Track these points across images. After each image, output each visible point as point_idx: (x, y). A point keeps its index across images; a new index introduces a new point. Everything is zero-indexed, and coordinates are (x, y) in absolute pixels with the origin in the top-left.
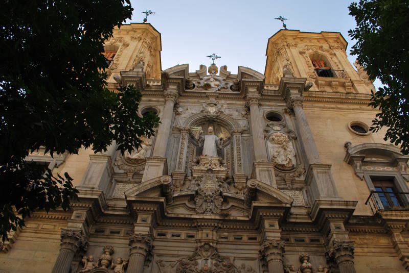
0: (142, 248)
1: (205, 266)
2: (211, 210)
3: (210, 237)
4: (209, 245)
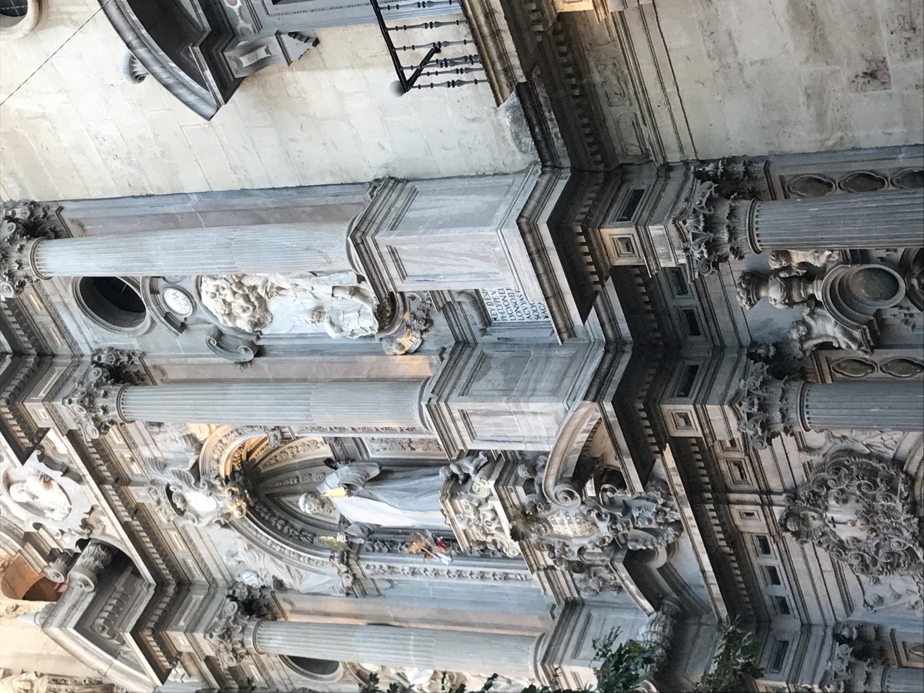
2: (657, 514)
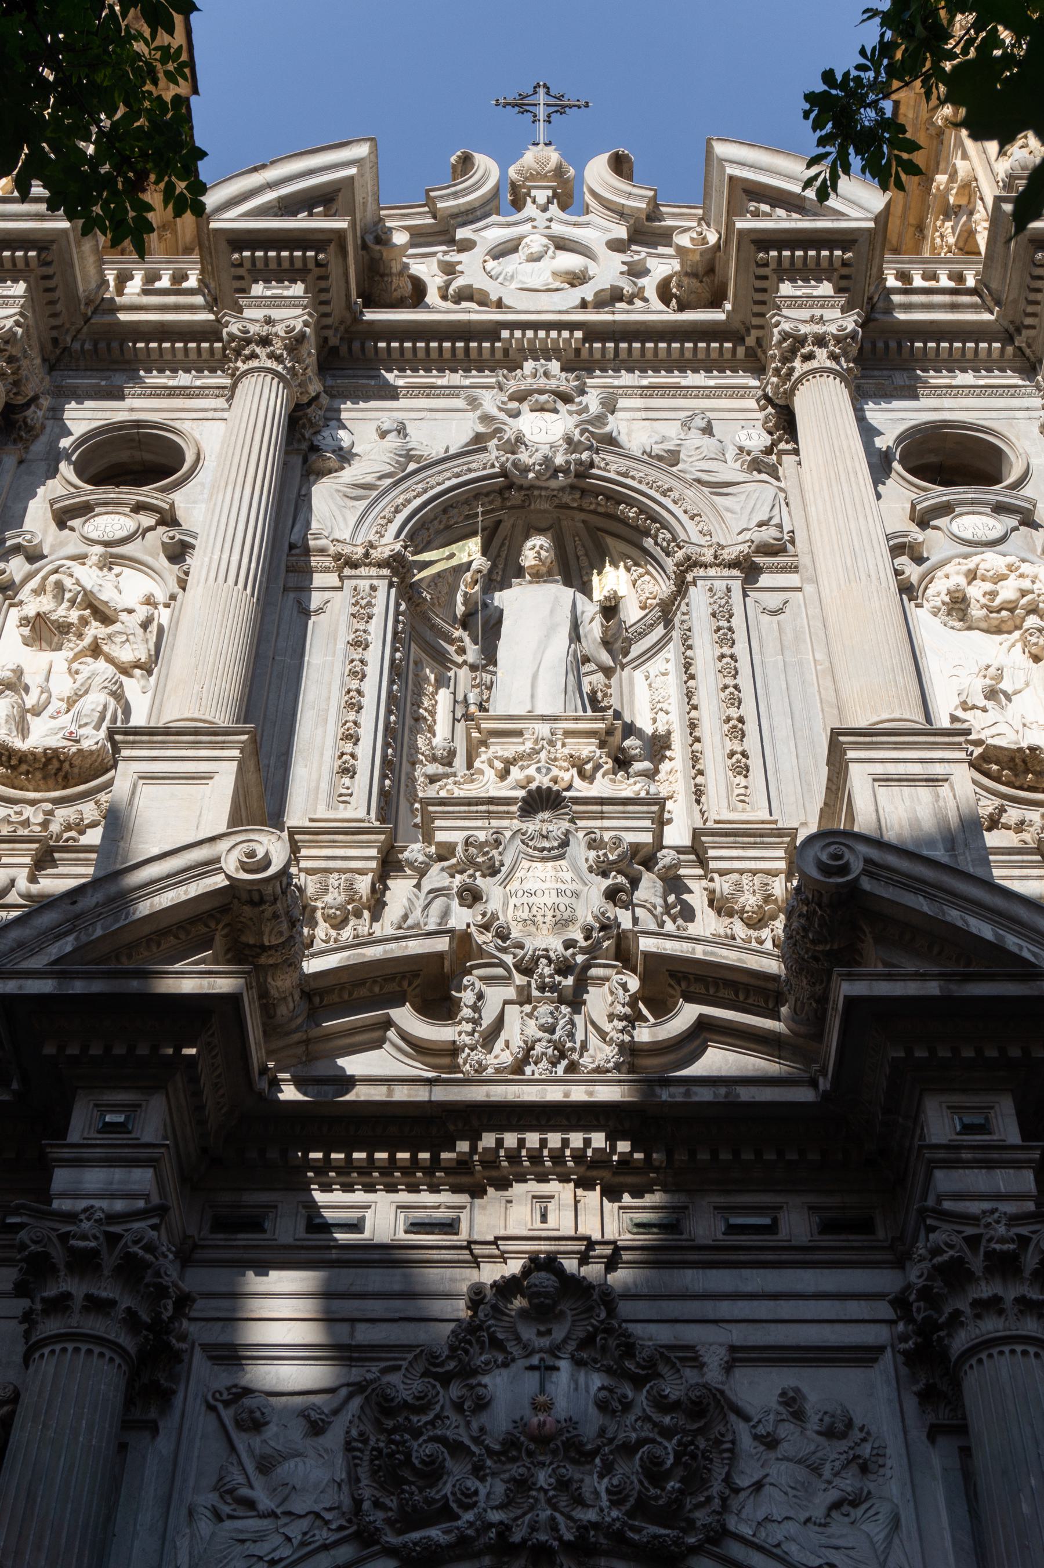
0: (96, 1305)
1: (536, 1407)
3: (561, 1221)
4: (559, 1272)
